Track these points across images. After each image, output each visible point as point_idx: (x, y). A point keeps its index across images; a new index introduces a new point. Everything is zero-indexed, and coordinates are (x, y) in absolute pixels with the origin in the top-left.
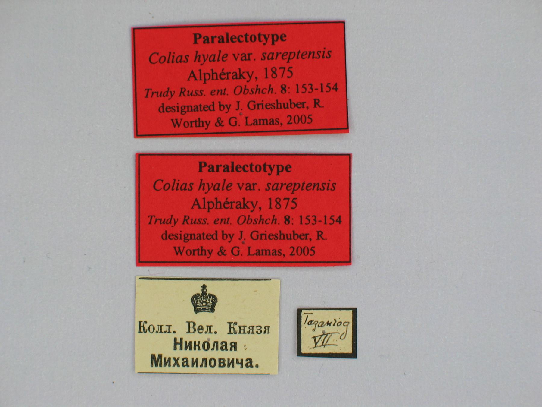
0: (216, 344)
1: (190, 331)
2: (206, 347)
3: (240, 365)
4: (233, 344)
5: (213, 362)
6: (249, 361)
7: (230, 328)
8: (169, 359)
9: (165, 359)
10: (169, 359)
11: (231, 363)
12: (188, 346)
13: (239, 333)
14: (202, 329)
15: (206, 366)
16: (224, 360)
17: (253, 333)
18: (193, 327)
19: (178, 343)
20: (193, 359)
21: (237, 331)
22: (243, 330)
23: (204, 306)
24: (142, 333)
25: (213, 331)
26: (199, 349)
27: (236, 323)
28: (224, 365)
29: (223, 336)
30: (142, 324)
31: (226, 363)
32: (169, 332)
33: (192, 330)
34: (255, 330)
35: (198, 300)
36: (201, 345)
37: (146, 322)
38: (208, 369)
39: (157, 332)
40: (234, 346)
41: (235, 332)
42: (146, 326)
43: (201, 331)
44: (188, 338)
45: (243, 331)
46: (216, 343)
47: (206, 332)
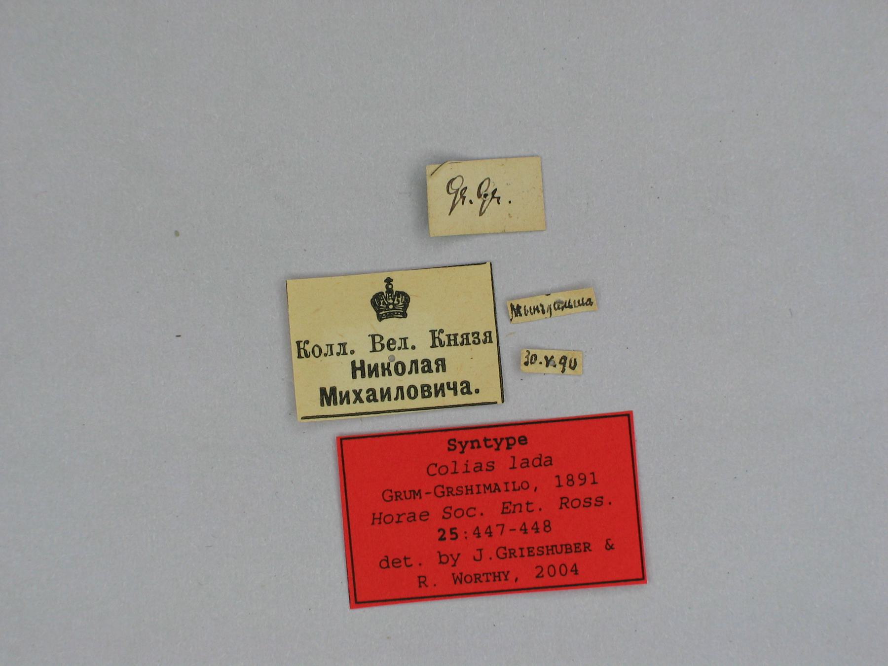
0: (414, 364)
1: (375, 349)
2: (400, 371)
3: (452, 392)
4: (440, 363)
5: (412, 391)
6: (464, 385)
7: (434, 338)
8: (348, 393)
9: (341, 393)
10: (348, 393)
11: (440, 390)
12: (373, 371)
13: (447, 346)
14: (394, 343)
15: (403, 398)
16: (429, 387)
17: (468, 344)
18: (379, 342)
19: (359, 369)
20: (382, 389)
21: (444, 342)
22: (453, 340)
23: (391, 310)
24: (437, 348)
25: (409, 346)
26: (390, 374)
27: (442, 331)
28: (430, 395)
29: (425, 351)
30: (302, 345)
31: (433, 390)
32: (345, 353)
33: (378, 347)
34: (471, 339)
35: (382, 302)
36: (392, 368)
37: (307, 342)
38: (407, 403)
39: (326, 355)
40: (441, 364)
41: (442, 342)
42: (309, 348)
43: (392, 347)
44: (372, 359)
45: (453, 341)
46: (414, 362)
47: (399, 348)
